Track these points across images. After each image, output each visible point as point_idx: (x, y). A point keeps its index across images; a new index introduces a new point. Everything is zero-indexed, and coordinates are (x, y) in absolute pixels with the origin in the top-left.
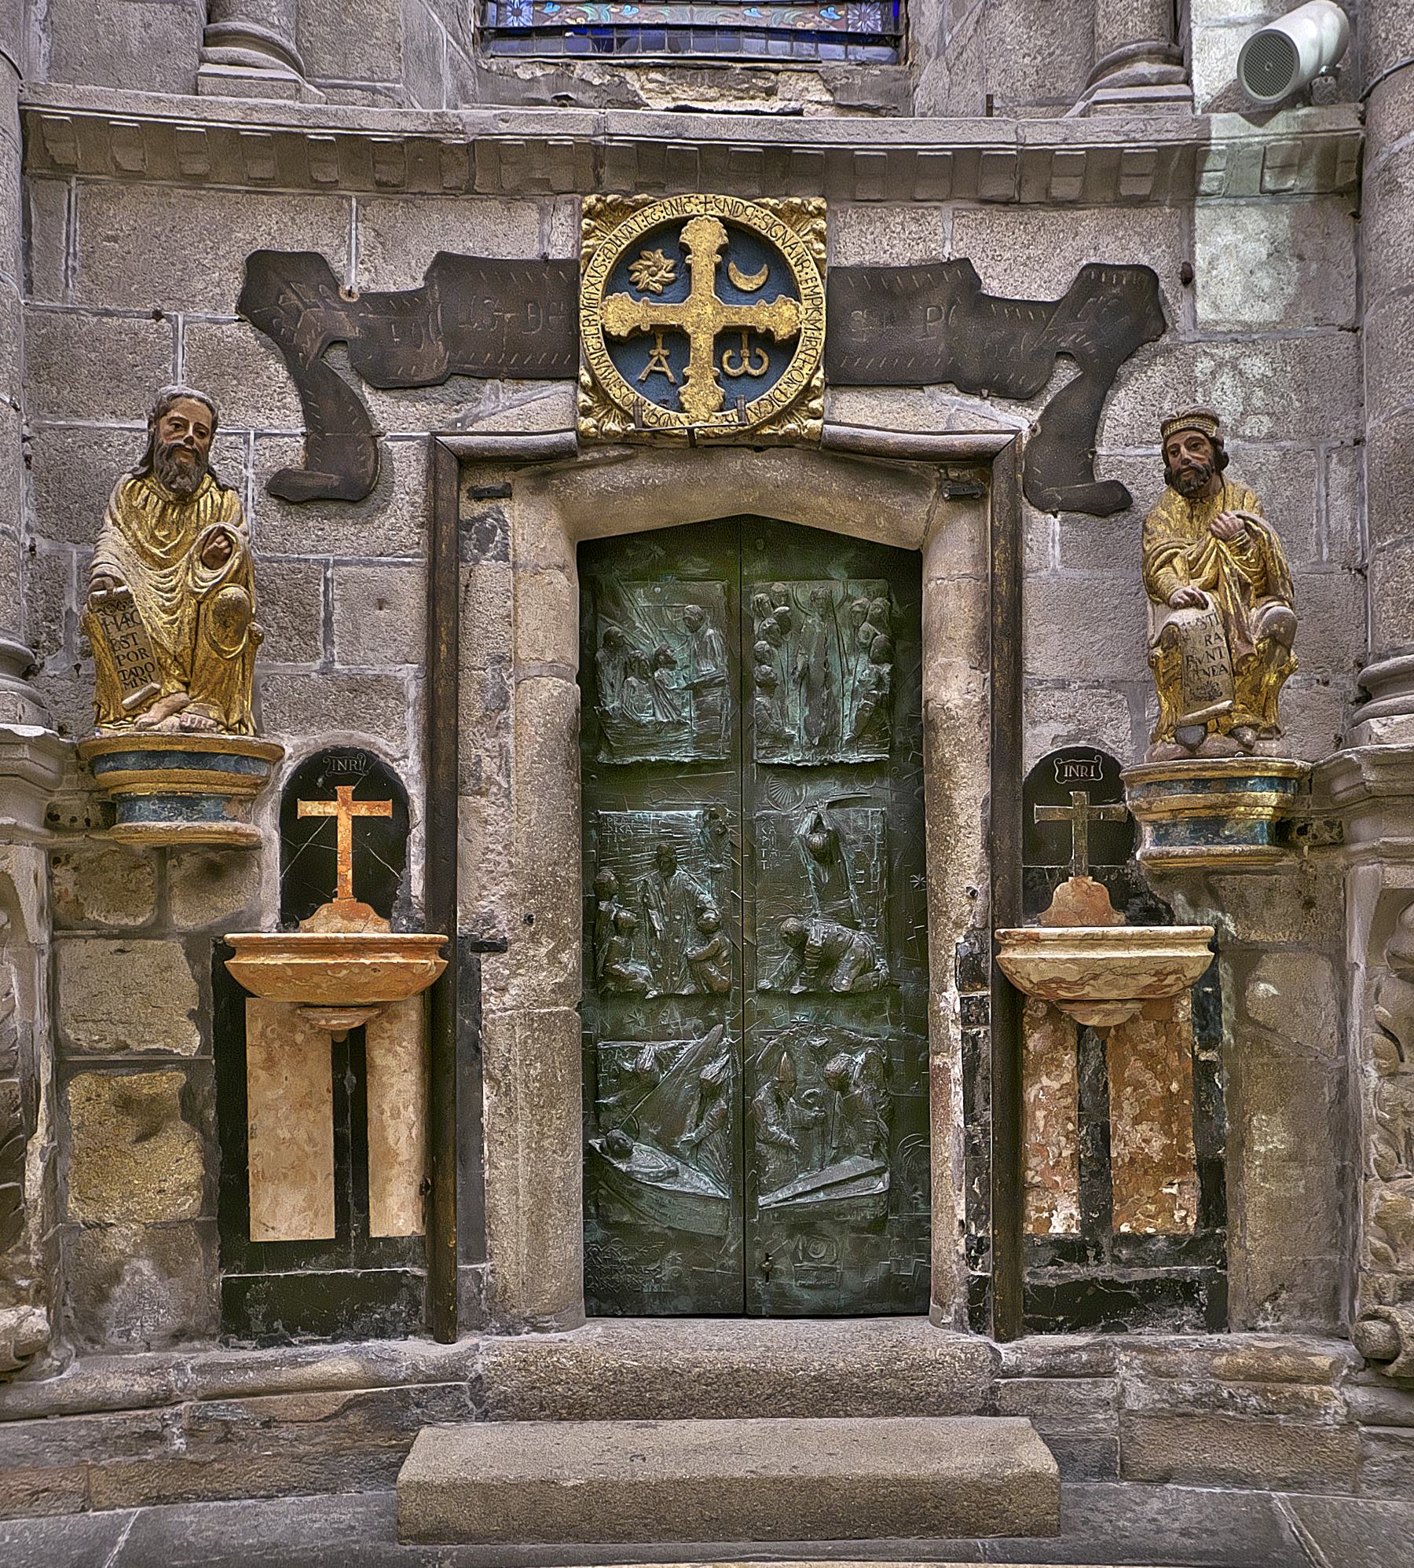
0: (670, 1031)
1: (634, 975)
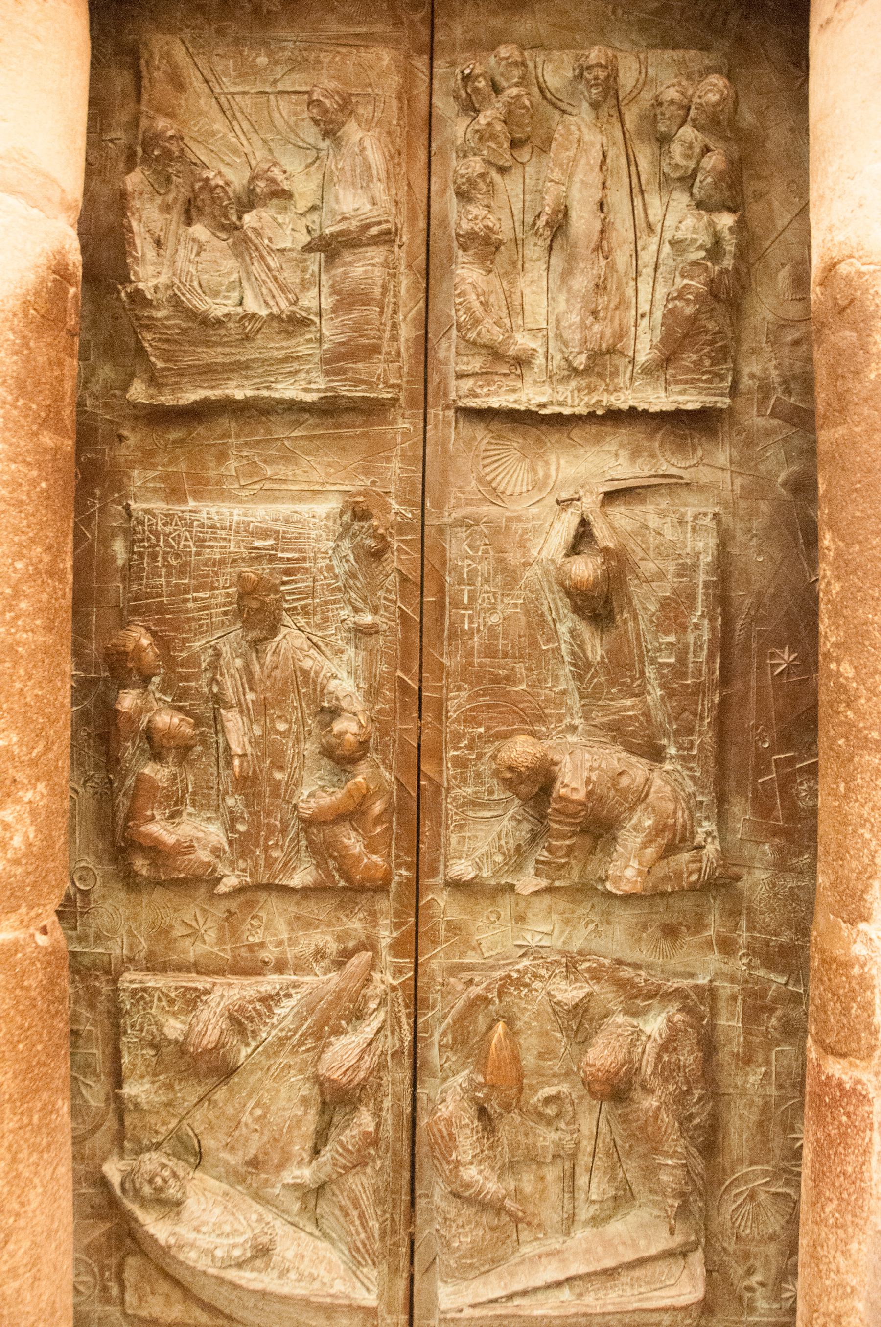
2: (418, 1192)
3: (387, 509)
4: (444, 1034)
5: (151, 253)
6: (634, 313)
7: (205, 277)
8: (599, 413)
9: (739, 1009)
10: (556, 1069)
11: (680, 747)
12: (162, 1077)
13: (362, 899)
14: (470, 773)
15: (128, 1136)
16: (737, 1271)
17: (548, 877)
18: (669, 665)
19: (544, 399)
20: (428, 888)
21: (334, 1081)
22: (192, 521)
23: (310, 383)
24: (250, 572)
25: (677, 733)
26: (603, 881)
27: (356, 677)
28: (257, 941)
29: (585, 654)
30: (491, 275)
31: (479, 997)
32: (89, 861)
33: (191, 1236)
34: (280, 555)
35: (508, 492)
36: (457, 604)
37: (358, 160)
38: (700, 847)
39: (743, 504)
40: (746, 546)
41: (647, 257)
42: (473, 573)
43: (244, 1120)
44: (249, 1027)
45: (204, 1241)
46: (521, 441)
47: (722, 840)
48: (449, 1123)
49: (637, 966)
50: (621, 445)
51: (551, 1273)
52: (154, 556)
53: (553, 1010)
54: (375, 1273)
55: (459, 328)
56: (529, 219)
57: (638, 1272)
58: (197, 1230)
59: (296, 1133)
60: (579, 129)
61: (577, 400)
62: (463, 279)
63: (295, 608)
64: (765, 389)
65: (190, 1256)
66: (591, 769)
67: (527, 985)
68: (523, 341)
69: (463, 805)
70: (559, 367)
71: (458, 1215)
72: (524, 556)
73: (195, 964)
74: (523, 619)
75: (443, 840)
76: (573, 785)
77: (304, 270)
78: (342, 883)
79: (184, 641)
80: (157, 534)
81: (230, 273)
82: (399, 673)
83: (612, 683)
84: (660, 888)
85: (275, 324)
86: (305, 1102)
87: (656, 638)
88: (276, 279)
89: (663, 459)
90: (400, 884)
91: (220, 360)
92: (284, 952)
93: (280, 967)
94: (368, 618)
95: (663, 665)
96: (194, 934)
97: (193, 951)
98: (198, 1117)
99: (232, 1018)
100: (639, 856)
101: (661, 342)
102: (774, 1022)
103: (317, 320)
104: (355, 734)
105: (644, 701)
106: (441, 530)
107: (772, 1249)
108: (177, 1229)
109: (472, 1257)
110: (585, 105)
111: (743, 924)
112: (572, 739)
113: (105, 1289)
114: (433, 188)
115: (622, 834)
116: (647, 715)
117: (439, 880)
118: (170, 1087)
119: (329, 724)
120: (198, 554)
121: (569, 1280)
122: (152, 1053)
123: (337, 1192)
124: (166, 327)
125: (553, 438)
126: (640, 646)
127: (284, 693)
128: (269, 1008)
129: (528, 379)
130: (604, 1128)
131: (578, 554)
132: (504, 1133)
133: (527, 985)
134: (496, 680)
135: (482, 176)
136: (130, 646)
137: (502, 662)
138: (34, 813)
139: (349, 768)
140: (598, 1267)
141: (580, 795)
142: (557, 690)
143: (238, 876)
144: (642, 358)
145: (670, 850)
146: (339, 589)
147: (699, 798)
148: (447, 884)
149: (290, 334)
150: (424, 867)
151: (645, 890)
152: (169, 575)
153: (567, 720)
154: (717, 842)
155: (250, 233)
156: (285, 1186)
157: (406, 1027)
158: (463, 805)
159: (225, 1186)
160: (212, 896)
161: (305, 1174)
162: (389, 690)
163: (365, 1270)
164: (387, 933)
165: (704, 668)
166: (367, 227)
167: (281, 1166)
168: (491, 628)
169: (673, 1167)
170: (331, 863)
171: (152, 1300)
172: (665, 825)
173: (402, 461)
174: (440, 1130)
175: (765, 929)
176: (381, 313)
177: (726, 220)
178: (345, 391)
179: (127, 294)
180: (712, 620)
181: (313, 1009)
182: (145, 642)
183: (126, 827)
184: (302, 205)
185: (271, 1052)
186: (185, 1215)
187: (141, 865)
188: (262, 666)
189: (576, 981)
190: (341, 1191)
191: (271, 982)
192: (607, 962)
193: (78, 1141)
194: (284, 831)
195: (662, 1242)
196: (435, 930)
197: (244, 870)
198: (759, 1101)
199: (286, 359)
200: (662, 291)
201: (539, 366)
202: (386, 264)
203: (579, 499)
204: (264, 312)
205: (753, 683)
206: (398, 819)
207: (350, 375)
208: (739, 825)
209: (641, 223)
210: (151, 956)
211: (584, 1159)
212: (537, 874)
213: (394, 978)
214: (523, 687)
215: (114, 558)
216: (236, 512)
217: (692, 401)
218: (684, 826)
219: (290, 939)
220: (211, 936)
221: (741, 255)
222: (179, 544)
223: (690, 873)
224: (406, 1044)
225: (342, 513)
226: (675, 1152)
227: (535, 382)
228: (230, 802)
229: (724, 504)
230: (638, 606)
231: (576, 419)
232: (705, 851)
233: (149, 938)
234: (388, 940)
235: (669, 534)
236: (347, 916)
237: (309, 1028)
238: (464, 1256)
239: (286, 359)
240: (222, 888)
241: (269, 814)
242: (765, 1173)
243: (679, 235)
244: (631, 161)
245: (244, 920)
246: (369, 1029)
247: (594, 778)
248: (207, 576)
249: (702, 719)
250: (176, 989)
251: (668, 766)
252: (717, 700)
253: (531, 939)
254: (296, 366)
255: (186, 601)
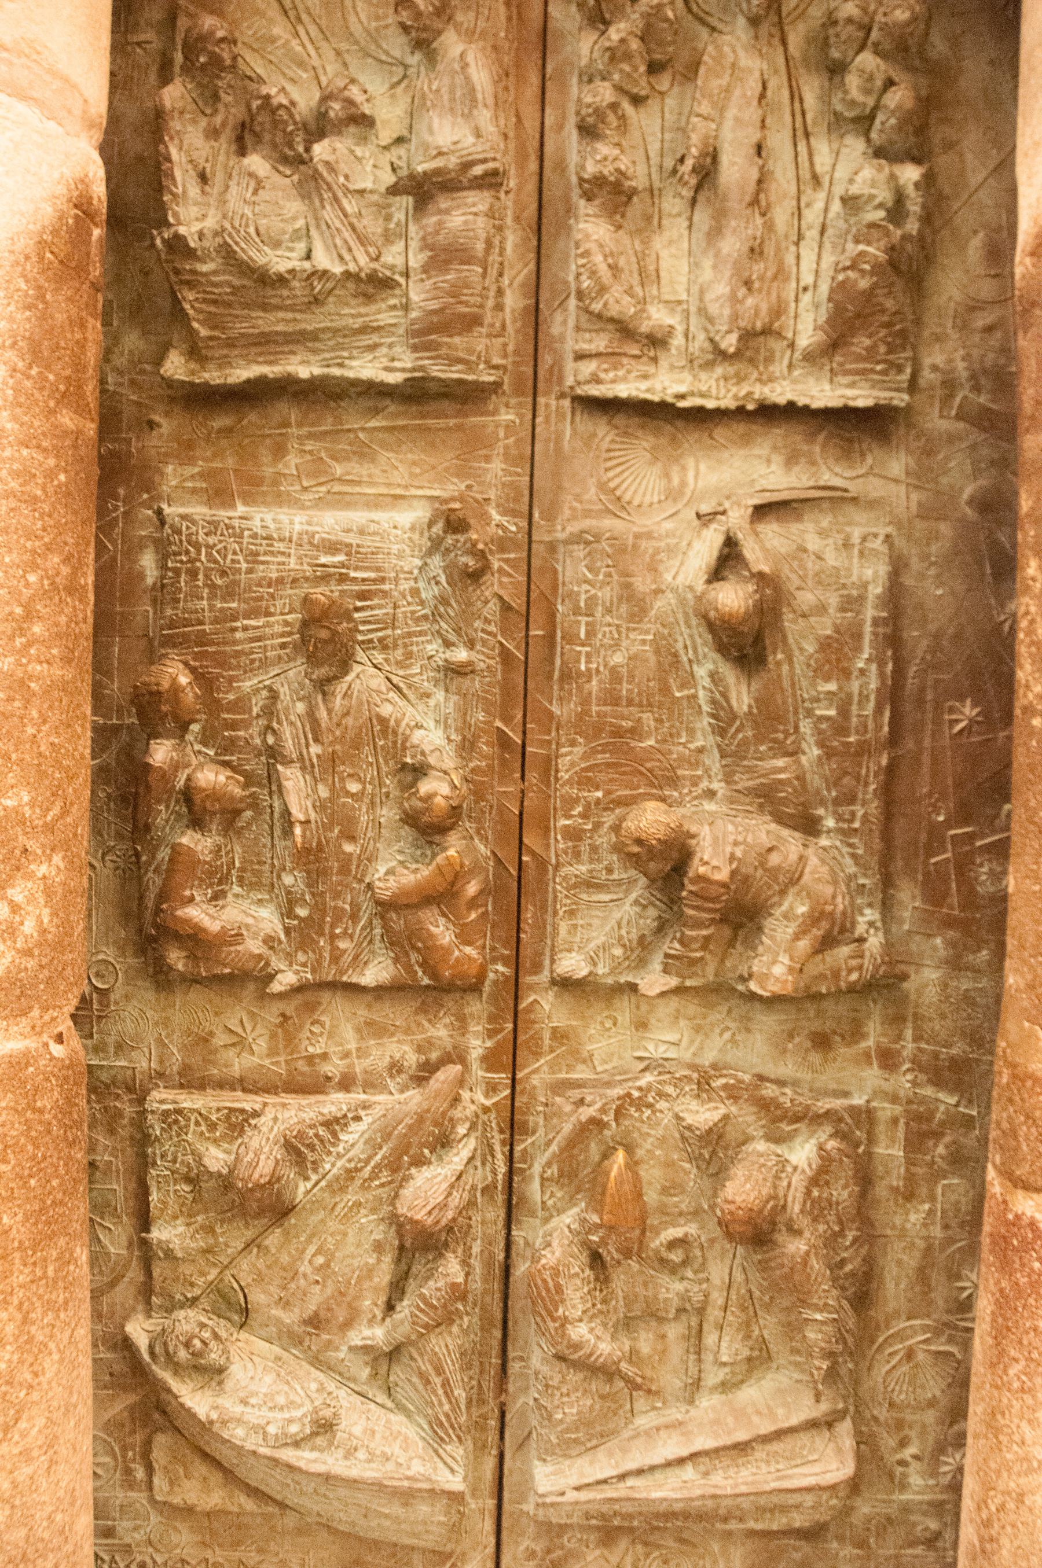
0: (327, 1069)
1: (233, 937)
2: (511, 1354)
3: (486, 519)
4: (549, 1164)
5: (194, 190)
6: (794, 285)
7: (263, 222)
8: (750, 407)
9: (901, 1134)
10: (683, 1206)
11: (840, 818)
12: (200, 1218)
13: (449, 1001)
14: (584, 848)
15: (157, 1289)
16: (888, 1441)
17: (678, 975)
18: (828, 718)
19: (682, 389)
20: (531, 988)
21: (417, 1222)
22: (242, 530)
23: (393, 360)
24: (320, 593)
25: (836, 802)
26: (743, 979)
27: (446, 727)
28: (319, 1051)
29: (728, 701)
30: (621, 232)
31: (592, 1120)
32: (109, 954)
33: (239, 1409)
34: (353, 574)
35: (636, 503)
36: (571, 638)
37: (459, 80)
38: (861, 940)
39: (920, 525)
40: (921, 576)
41: (812, 216)
42: (591, 601)
43: (302, 1269)
44: (310, 1156)
45: (253, 1416)
46: (652, 439)
47: (887, 932)
48: (556, 1272)
49: (780, 1083)
50: (775, 448)
51: (671, 1448)
52: (193, 574)
53: (682, 1136)
54: (461, 1452)
55: (580, 295)
56: (669, 163)
57: (775, 1446)
58: (244, 1402)
59: (366, 1285)
60: (734, 51)
61: (723, 391)
62: (587, 236)
63: (371, 641)
64: (950, 385)
65: (237, 1434)
66: (736, 843)
67: (650, 1106)
68: (658, 317)
69: (575, 886)
70: (702, 350)
71: (563, 1381)
72: (655, 581)
73: (241, 1080)
74: (652, 659)
75: (549, 928)
76: (715, 863)
77: (388, 218)
78: (426, 981)
79: (231, 680)
80: (197, 546)
81: (294, 219)
82: (498, 724)
83: (759, 739)
84: (814, 989)
85: (351, 285)
86: (378, 1247)
87: (814, 685)
88: (354, 229)
89: (824, 468)
90: (495, 983)
91: (280, 328)
92: (351, 1066)
93: (346, 1084)
94: (461, 655)
95: (821, 719)
96: (240, 1043)
97: (238, 1064)
98: (245, 1267)
99: (288, 1146)
100: (790, 950)
101: (827, 322)
102: (941, 1150)
103: (402, 280)
104: (446, 798)
105: (798, 762)
106: (552, 547)
107: (930, 1417)
108: (220, 1401)
109: (577, 1430)
110: (741, 21)
111: (909, 1033)
112: (709, 806)
113: (128, 1471)
114: (548, 122)
115: (769, 923)
116: (801, 778)
117: (544, 977)
118: (209, 1230)
119: (414, 784)
120: (250, 571)
121: (694, 1456)
122: (187, 1188)
123: (415, 1355)
124: (216, 285)
125: (692, 437)
126: (794, 695)
127: (357, 745)
128: (334, 1134)
129: (664, 363)
130: (739, 1277)
131: (723, 579)
132: (619, 1282)
133: (650, 1106)
134: (618, 733)
135: (614, 106)
136: (166, 685)
137: (625, 711)
138: (48, 892)
139: (437, 838)
140: (728, 1441)
141: (722, 875)
142: (692, 746)
143: (297, 972)
144: (804, 341)
145: (827, 943)
146: (425, 617)
147: (862, 881)
148: (554, 982)
149: (368, 298)
150: (526, 963)
151: (796, 990)
152: (212, 596)
153: (704, 784)
154: (881, 934)
155: (321, 168)
156: (351, 1349)
157: (499, 1156)
158: (575, 886)
159: (277, 1350)
160: (264, 997)
161: (377, 1334)
162: (487, 744)
163: (448, 1448)
164: (479, 1042)
165: (871, 725)
166: (467, 166)
167: (348, 1324)
168: (614, 670)
169: (823, 1323)
170: (414, 957)
171: (187, 1484)
172: (822, 913)
173: (505, 462)
174: (544, 1281)
175: (932, 1040)
176: (484, 275)
177: (910, 174)
178: (438, 371)
179: (163, 240)
180: (881, 665)
181: (390, 1134)
182: (184, 680)
183: (158, 911)
184: (386, 136)
185: (336, 1187)
186: (229, 1385)
187: (176, 958)
188: (330, 711)
189: (710, 1100)
190: (421, 1355)
191: (335, 1103)
192: (747, 1078)
193: (96, 1295)
194: (354, 917)
195: (806, 1409)
196: (537, 1038)
197: (304, 965)
198: (921, 1244)
199: (364, 330)
200: (828, 260)
201: (678, 348)
202: (490, 214)
203: (724, 513)
204: (338, 269)
205: (927, 743)
206: (494, 903)
207: (443, 351)
208: (907, 914)
209: (805, 174)
210: (185, 1070)
211: (714, 1314)
212: (666, 971)
213: (487, 1096)
214: (651, 742)
215: (141, 576)
216: (297, 519)
217: (862, 397)
218: (844, 913)
219: (359, 1049)
220: (262, 1045)
221: (927, 218)
222: (225, 558)
223: (850, 971)
224: (500, 1177)
225: (431, 524)
226: (826, 1304)
227: (672, 367)
228: (288, 880)
229: (898, 524)
230: (794, 647)
231: (720, 415)
232: (867, 945)
233: (183, 1048)
234: (480, 1051)
235: (832, 559)
236: (430, 1021)
237: (384, 1158)
238: (567, 1430)
239: (364, 330)
240: (276, 987)
241: (337, 895)
242: (925, 1329)
243: (854, 190)
244: (796, 95)
245: (302, 1026)
246: (458, 1157)
247: (739, 854)
248: (260, 599)
249: (866, 784)
250: (218, 1110)
251: (824, 841)
252: (884, 761)
253: (655, 1050)
254: (375, 338)
255: (234, 630)
